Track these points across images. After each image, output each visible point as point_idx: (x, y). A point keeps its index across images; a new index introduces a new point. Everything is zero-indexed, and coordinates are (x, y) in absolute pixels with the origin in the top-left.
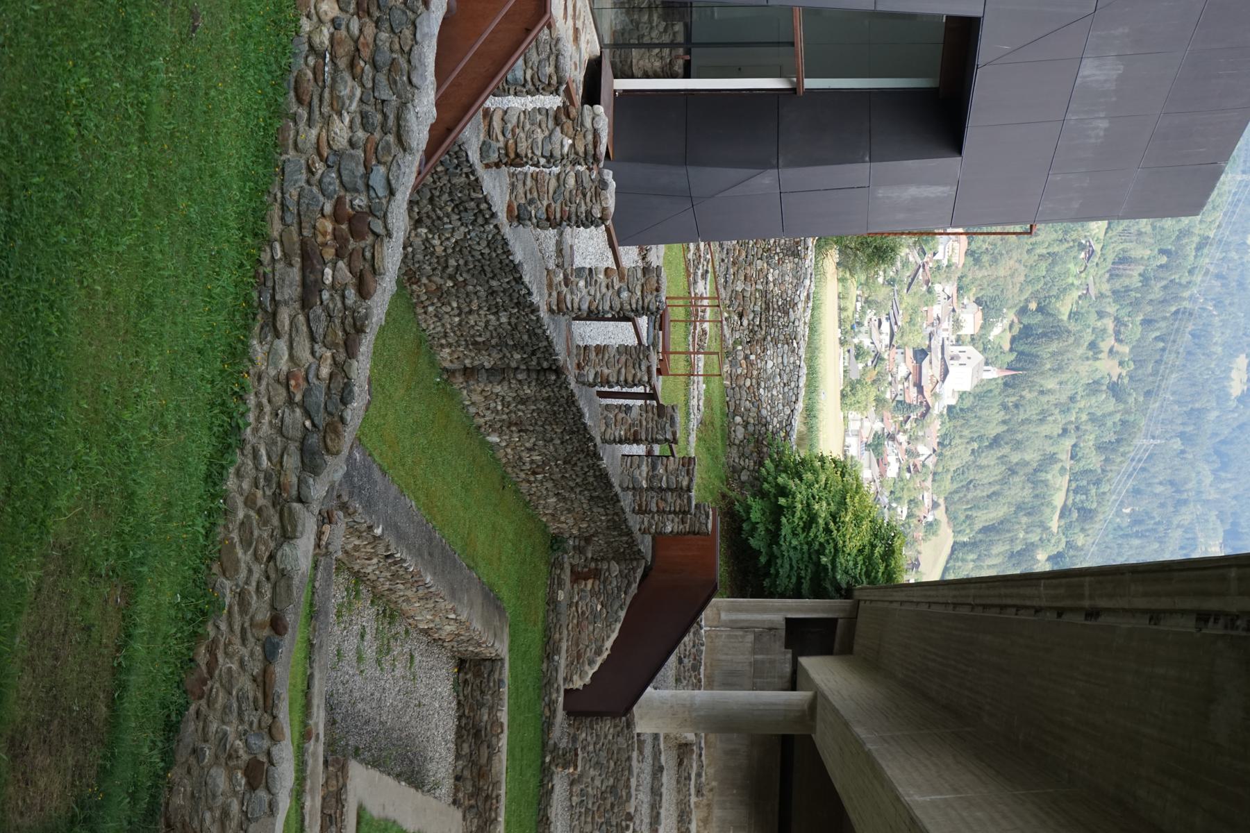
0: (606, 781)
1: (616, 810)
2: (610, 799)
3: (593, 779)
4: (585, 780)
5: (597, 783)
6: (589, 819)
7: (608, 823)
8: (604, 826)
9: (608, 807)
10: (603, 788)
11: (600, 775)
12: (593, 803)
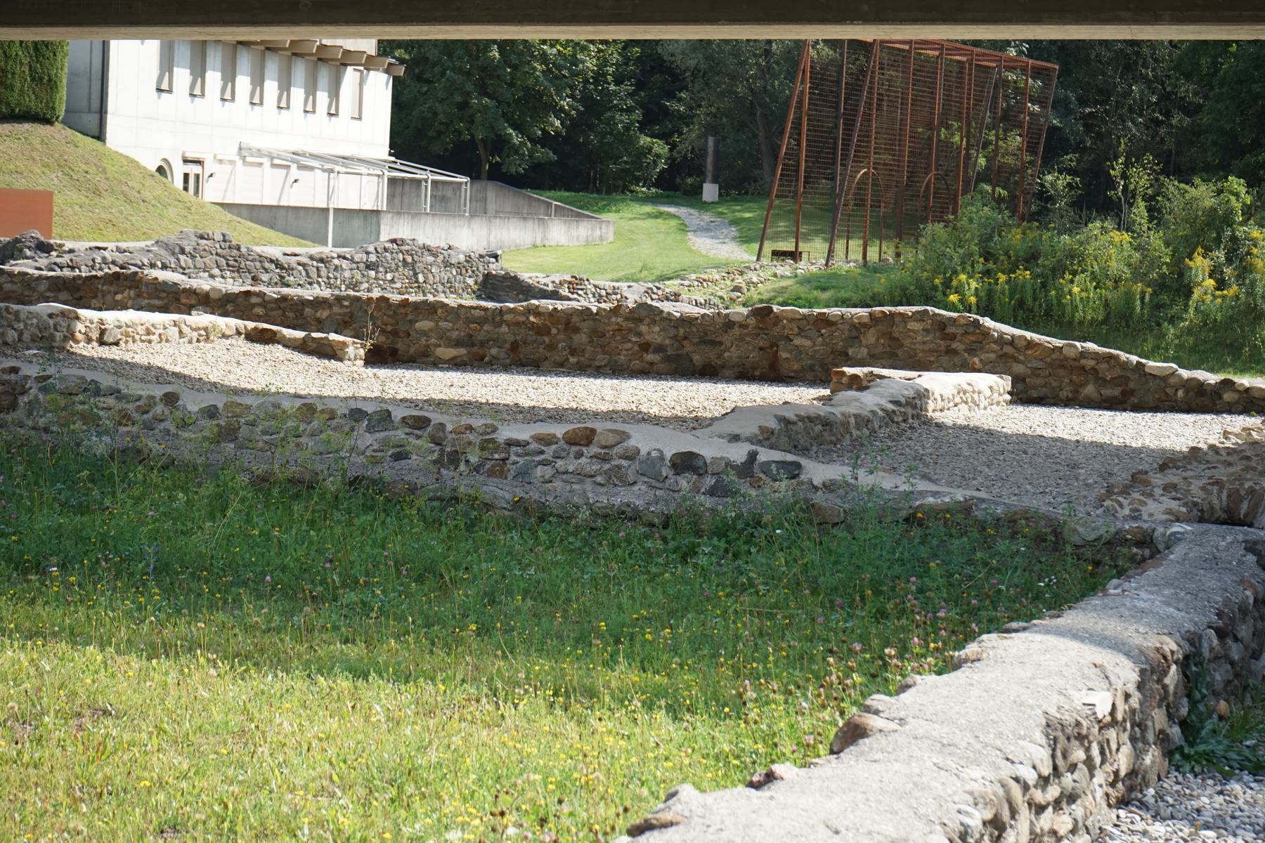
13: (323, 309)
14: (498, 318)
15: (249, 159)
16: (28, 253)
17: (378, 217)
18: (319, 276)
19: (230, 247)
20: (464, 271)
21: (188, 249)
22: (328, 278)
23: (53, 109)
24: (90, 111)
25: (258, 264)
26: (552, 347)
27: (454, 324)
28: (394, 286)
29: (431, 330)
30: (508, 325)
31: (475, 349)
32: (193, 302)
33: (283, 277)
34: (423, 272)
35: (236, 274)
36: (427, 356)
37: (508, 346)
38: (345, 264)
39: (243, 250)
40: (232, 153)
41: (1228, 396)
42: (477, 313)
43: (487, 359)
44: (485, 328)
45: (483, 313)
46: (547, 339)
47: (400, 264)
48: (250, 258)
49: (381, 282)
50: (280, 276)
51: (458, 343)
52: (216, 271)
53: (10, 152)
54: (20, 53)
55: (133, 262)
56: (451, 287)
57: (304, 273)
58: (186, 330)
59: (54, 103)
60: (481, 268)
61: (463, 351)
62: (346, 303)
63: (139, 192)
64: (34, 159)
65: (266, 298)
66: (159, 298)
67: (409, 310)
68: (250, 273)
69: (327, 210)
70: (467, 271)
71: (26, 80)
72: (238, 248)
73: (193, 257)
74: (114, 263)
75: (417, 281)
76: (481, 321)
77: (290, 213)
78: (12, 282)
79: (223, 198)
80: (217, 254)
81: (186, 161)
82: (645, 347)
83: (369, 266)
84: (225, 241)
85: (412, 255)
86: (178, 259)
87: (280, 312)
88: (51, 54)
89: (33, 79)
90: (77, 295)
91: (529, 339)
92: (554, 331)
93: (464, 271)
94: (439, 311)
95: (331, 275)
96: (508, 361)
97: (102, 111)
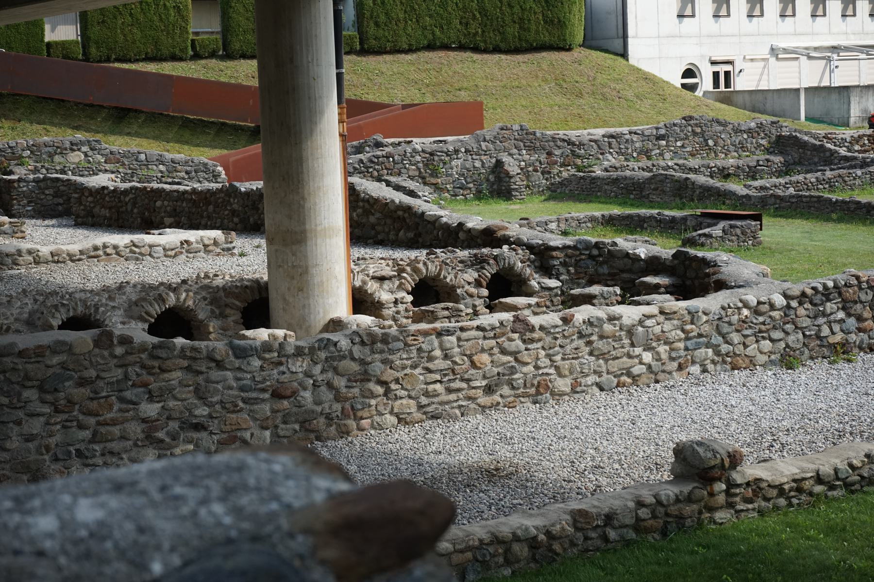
0: (32, 407)
1: (93, 373)
2: (70, 389)
3: (29, 438)
4: (32, 457)
5: (36, 426)
6: (116, 430)
7: (119, 387)
8: (128, 394)
9: (86, 391)
10: (47, 410)
11: (19, 423)
12: (81, 427)
15: (780, 56)
16: (367, 149)
17: (847, 91)
18: (610, 148)
19: (526, 134)
20: (755, 135)
21: (487, 138)
22: (620, 148)
23: (565, 40)
24: (618, 38)
25: (552, 144)
28: (684, 150)
31: (177, 219)
33: (575, 151)
34: (711, 138)
35: (532, 152)
38: (635, 138)
39: (538, 135)
40: (765, 52)
41: (461, 235)
47: (689, 134)
48: (544, 140)
49: (673, 148)
50: (571, 151)
51: (170, 216)
52: (515, 151)
53: (521, 74)
54: (534, 6)
56: (743, 147)
57: (595, 147)
59: (564, 36)
60: (774, 131)
63: (619, 92)
64: (537, 77)
66: (77, 193)
68: (544, 150)
69: (797, 90)
70: (759, 134)
71: (540, 23)
72: (534, 134)
73: (493, 143)
74: (423, 151)
75: (707, 145)
77: (775, 94)
78: (63, 185)
79: (758, 85)
80: (515, 139)
81: (713, 63)
82: (234, 213)
83: (659, 138)
84: (522, 129)
85: (701, 127)
86: (480, 145)
88: (559, 4)
89: (546, 22)
93: (755, 135)
95: (622, 146)
97: (625, 37)
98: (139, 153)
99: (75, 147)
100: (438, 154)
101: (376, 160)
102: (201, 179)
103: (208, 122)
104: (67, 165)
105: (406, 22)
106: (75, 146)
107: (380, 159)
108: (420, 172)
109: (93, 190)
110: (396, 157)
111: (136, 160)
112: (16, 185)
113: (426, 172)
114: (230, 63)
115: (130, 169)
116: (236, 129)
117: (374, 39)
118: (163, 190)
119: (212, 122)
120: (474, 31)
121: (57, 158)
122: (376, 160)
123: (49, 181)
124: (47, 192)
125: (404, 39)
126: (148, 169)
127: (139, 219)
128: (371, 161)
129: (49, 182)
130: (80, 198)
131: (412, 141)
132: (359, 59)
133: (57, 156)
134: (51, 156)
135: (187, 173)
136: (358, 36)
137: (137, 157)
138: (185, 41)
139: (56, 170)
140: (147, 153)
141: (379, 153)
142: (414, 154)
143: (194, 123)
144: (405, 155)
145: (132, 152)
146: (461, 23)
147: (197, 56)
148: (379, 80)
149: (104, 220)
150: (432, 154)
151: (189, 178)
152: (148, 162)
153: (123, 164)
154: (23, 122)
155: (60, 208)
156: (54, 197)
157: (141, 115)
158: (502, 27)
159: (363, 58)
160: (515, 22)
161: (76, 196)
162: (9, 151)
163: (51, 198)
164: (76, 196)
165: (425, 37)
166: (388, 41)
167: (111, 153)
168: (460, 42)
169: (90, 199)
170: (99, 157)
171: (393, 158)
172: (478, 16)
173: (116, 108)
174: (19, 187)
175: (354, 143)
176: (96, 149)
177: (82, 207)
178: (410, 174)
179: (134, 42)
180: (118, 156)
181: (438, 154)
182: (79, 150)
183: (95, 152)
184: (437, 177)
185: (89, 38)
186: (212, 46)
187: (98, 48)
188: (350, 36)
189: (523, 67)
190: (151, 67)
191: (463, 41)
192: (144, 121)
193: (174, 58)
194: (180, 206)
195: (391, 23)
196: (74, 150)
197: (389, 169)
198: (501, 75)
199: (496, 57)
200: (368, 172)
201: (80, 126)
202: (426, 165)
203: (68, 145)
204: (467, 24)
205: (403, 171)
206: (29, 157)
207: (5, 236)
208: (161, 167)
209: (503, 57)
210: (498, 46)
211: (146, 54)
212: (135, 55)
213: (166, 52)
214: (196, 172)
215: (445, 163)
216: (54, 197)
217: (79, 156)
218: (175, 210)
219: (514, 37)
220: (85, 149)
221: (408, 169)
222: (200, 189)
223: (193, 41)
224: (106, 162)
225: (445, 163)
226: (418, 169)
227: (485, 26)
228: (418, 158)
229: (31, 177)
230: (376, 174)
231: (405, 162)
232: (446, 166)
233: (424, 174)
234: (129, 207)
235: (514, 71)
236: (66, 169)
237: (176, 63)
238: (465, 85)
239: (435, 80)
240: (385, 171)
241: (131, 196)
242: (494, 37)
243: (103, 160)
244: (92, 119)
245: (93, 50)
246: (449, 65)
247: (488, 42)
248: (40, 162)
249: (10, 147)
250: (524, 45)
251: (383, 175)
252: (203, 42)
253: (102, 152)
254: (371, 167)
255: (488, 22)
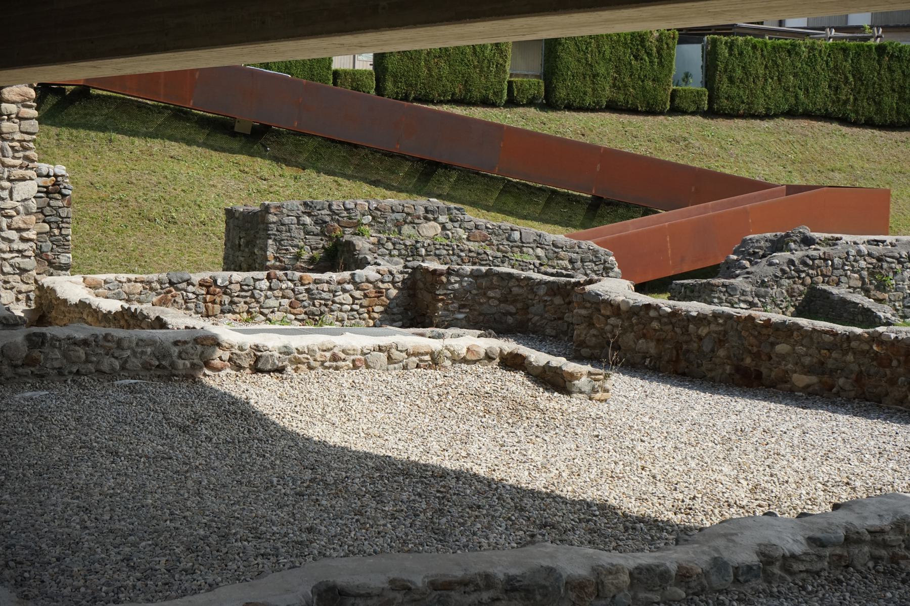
13: (704, 325)
14: (845, 345)
16: (792, 245)
26: (893, 382)
27: (808, 348)
29: (788, 354)
30: (854, 353)
31: (825, 378)
32: (608, 313)
36: (786, 382)
37: (853, 376)
42: (828, 338)
43: (834, 390)
44: (834, 355)
45: (832, 338)
46: (888, 371)
51: (808, 370)
53: (901, 156)
55: (890, 254)
58: (396, 354)
61: (813, 379)
62: (721, 321)
65: (661, 312)
66: (585, 308)
67: (770, 331)
74: (870, 255)
76: (831, 348)
78: (519, 286)
87: (671, 326)
90: (567, 300)
91: (872, 371)
92: (895, 363)
94: (795, 333)
96: (853, 394)
98: (512, 230)
99: (430, 216)
100: (889, 259)
101: (811, 263)
102: (588, 272)
103: (535, 188)
104: (420, 239)
105: (766, 80)
106: (430, 214)
107: (816, 262)
108: (864, 283)
109: (623, 307)
110: (836, 260)
111: (508, 239)
112: (444, 279)
113: (871, 284)
114: (552, 115)
115: (498, 250)
116: (570, 199)
117: (727, 99)
118: (799, 328)
119: (540, 189)
120: (844, 98)
121: (407, 229)
122: (811, 263)
123: (495, 278)
124: (491, 294)
125: (762, 101)
126: (522, 252)
127: (728, 368)
128: (805, 264)
129: (495, 278)
130: (590, 318)
131: (841, 239)
132: (706, 121)
133: (406, 226)
134: (398, 225)
135: (571, 261)
136: (707, 93)
137: (510, 235)
138: (500, 83)
139: (406, 246)
140: (523, 231)
141: (815, 253)
142: (858, 258)
143: (518, 189)
144: (847, 259)
145: (503, 227)
146: (830, 87)
147: (512, 103)
148: (735, 150)
149: (645, 358)
150: (879, 259)
151: (573, 269)
152: (522, 242)
153: (491, 244)
154: (308, 171)
155: (510, 320)
156: (500, 301)
157: (454, 172)
158: (878, 95)
159: (710, 121)
160: (894, 91)
161: (583, 312)
162: (345, 214)
163: (496, 302)
164: (583, 312)
165: (787, 100)
166: (743, 102)
167: (477, 227)
168: (827, 110)
169: (612, 320)
170: (461, 231)
171: (832, 261)
172: (851, 79)
173: (422, 160)
174: (449, 282)
175: (768, 235)
176: (457, 221)
177: (593, 332)
178: (851, 285)
179: (439, 79)
180: (485, 232)
181: (889, 259)
182: (435, 220)
183: (456, 224)
184: (884, 290)
185: (386, 69)
186: (532, 92)
187: (395, 83)
188: (698, 92)
189: (902, 147)
190: (459, 111)
191: (830, 110)
192: (458, 179)
193: (486, 103)
194: (836, 359)
195: (748, 80)
196: (430, 220)
197: (826, 276)
198: (878, 156)
199: (868, 132)
200: (799, 277)
201: (379, 181)
202: (872, 274)
203: (421, 212)
204: (837, 88)
205: (843, 279)
206: (370, 225)
207: (581, 396)
208: (540, 252)
209: (877, 132)
210: (871, 119)
211: (453, 94)
212: (439, 95)
213: (476, 94)
214: (582, 261)
215: (895, 273)
216: (500, 301)
217: (435, 228)
218: (822, 363)
219: (892, 109)
220: (443, 218)
221: (849, 278)
222: (893, 336)
223: (510, 83)
224: (468, 239)
225: (895, 273)
226: (862, 278)
227: (859, 93)
228: (863, 264)
229: (468, 268)
230: (808, 281)
231: (847, 268)
232: (898, 277)
233: (868, 286)
234: (707, 346)
235: (893, 152)
236: (419, 245)
237: (488, 109)
238: (838, 165)
239: (801, 156)
240: (821, 278)
241: (713, 327)
242: (868, 107)
243: (465, 237)
244: (393, 173)
245: (389, 85)
246: (816, 140)
247: (860, 112)
248: (384, 232)
249: (346, 209)
250: (903, 120)
251: (817, 283)
252: (521, 85)
253: (466, 225)
254: (804, 271)
255: (863, 89)
